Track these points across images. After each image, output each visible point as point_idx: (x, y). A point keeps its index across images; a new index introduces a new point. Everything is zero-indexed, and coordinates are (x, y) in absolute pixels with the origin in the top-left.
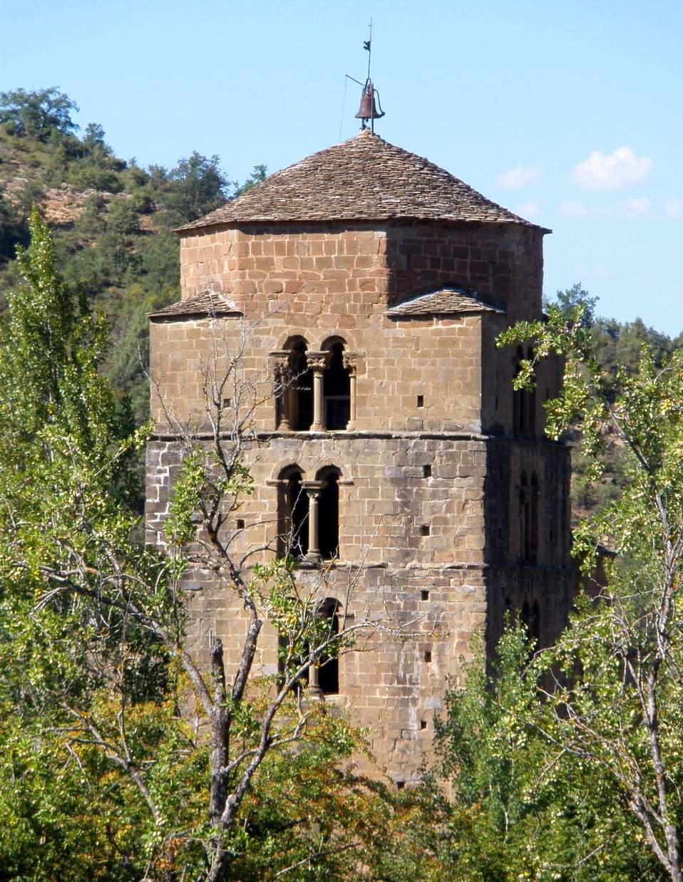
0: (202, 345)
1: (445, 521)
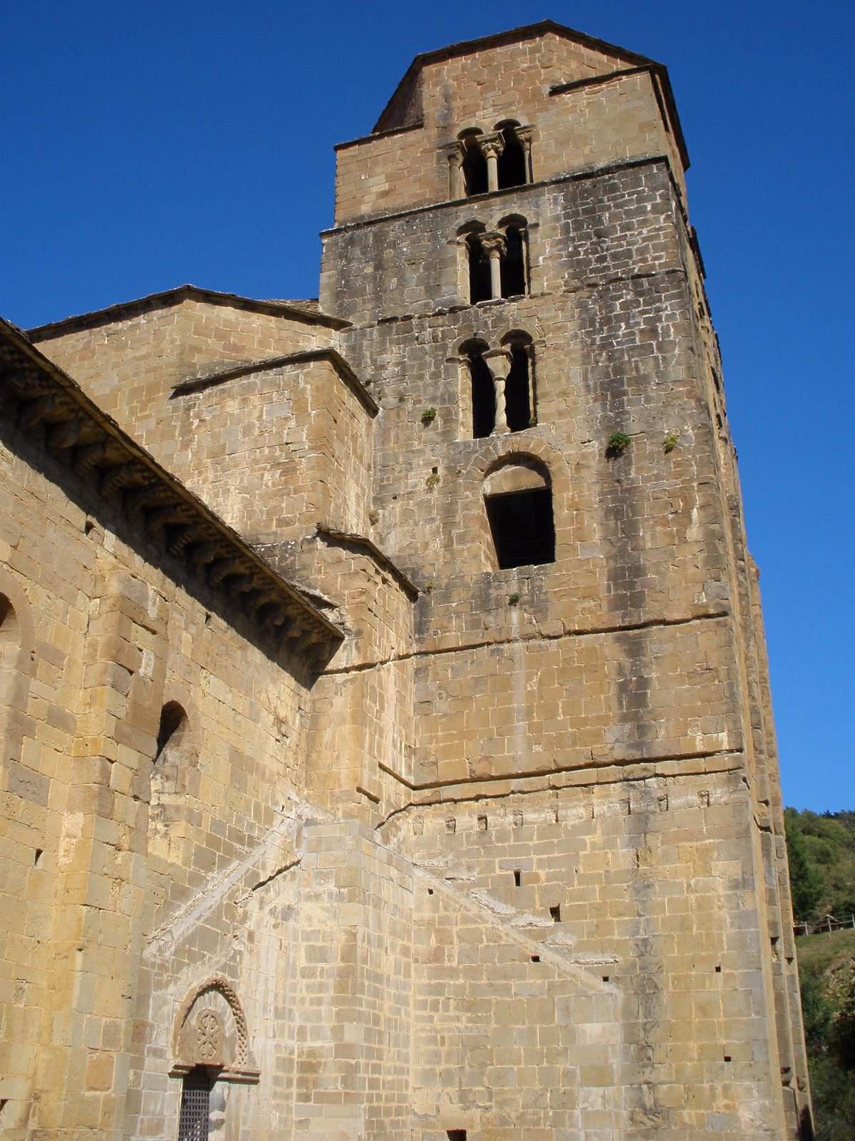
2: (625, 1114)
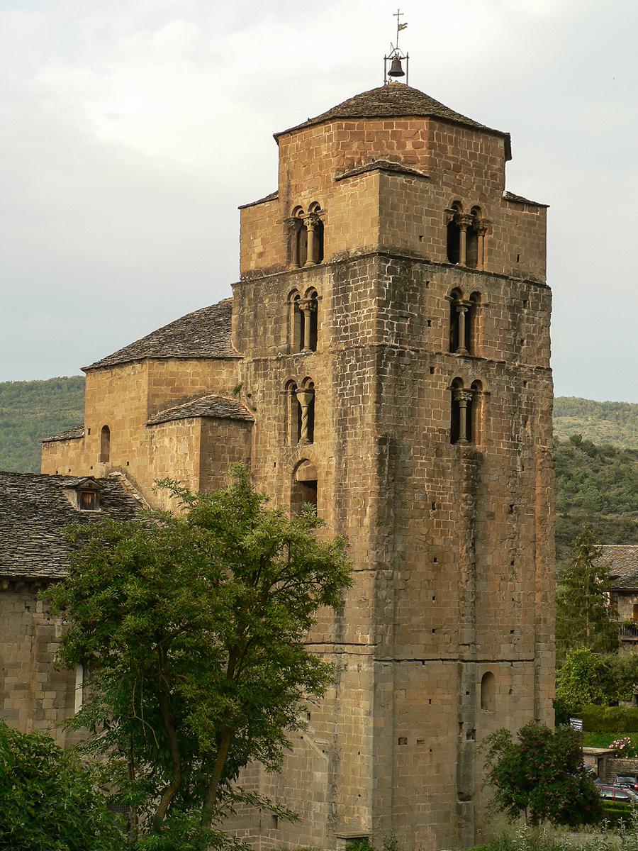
0: (408, 195)
1: (533, 338)
2: (327, 815)
